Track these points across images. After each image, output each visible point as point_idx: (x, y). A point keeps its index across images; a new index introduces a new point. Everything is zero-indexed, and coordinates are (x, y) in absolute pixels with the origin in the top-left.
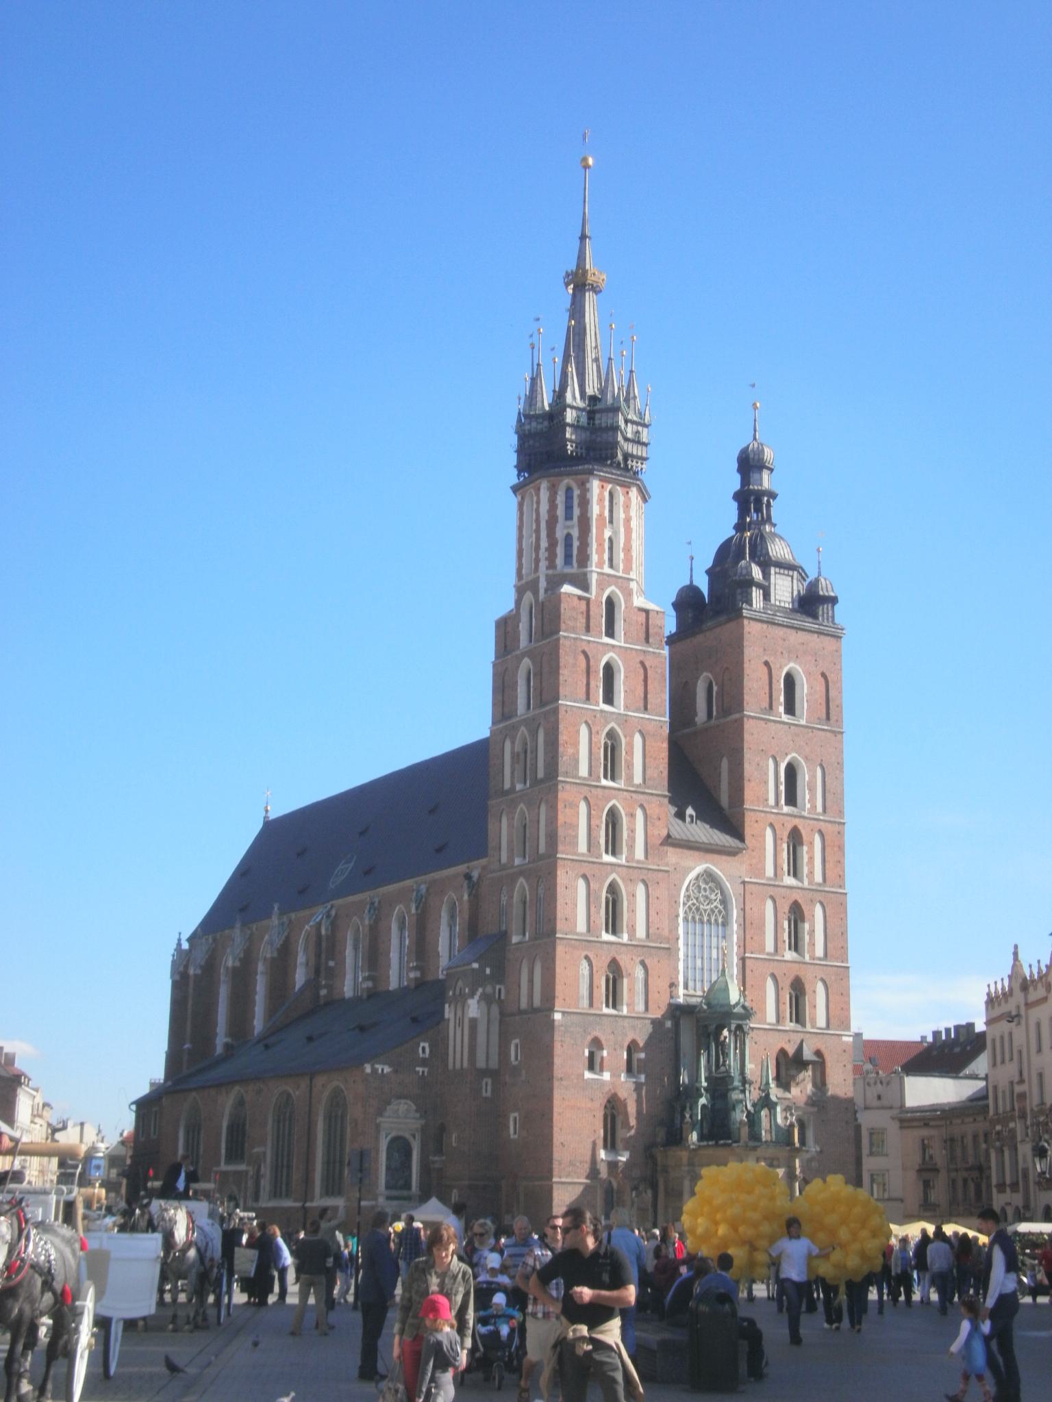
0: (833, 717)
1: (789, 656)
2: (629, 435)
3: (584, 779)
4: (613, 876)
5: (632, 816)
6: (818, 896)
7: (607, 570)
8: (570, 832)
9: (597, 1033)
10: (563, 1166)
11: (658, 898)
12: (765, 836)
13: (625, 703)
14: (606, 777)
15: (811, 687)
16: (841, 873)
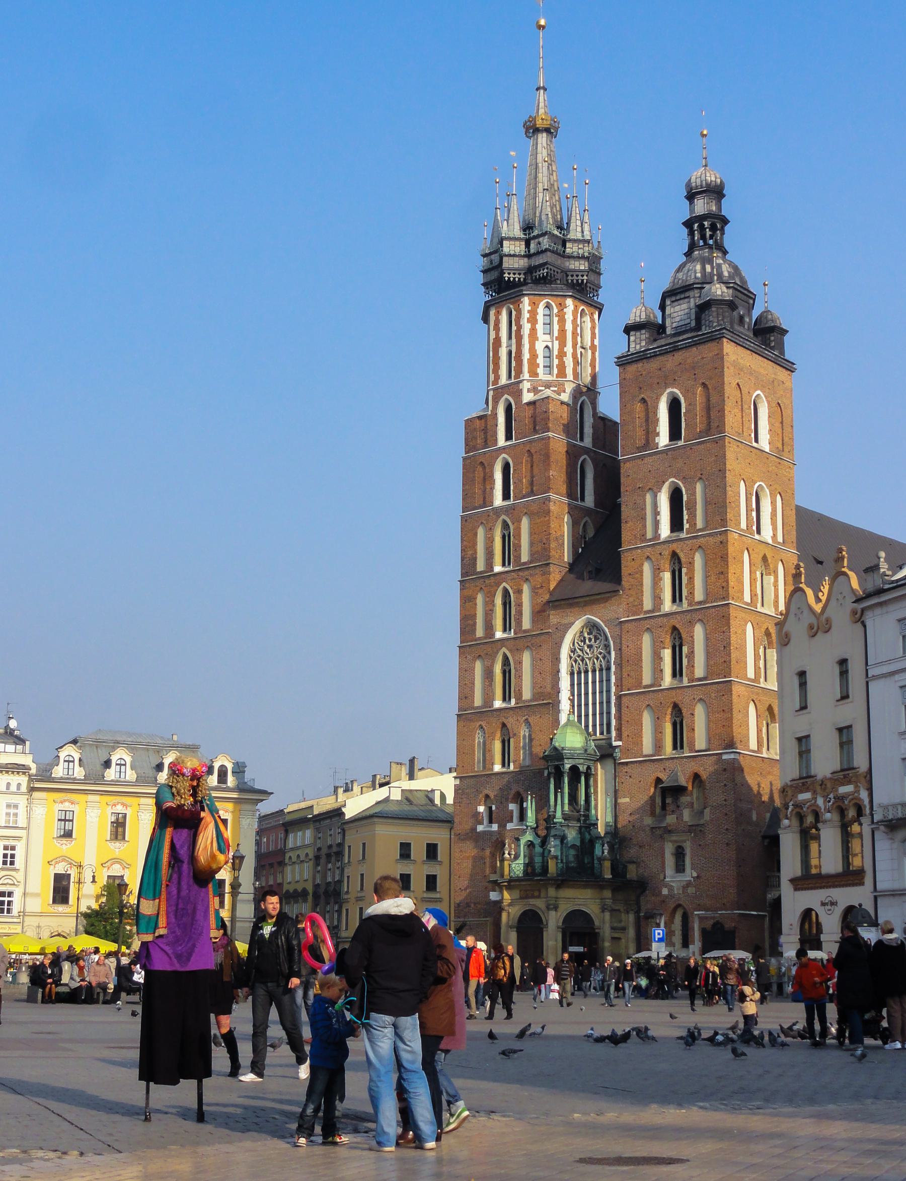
0: (714, 425)
1: (665, 383)
2: (532, 251)
3: (481, 572)
4: (504, 650)
5: (519, 592)
6: (697, 616)
7: (503, 380)
8: (470, 622)
9: (487, 792)
10: (461, 908)
11: (540, 659)
12: (641, 572)
13: (514, 494)
14: (504, 565)
15: (689, 405)
16: (723, 584)
